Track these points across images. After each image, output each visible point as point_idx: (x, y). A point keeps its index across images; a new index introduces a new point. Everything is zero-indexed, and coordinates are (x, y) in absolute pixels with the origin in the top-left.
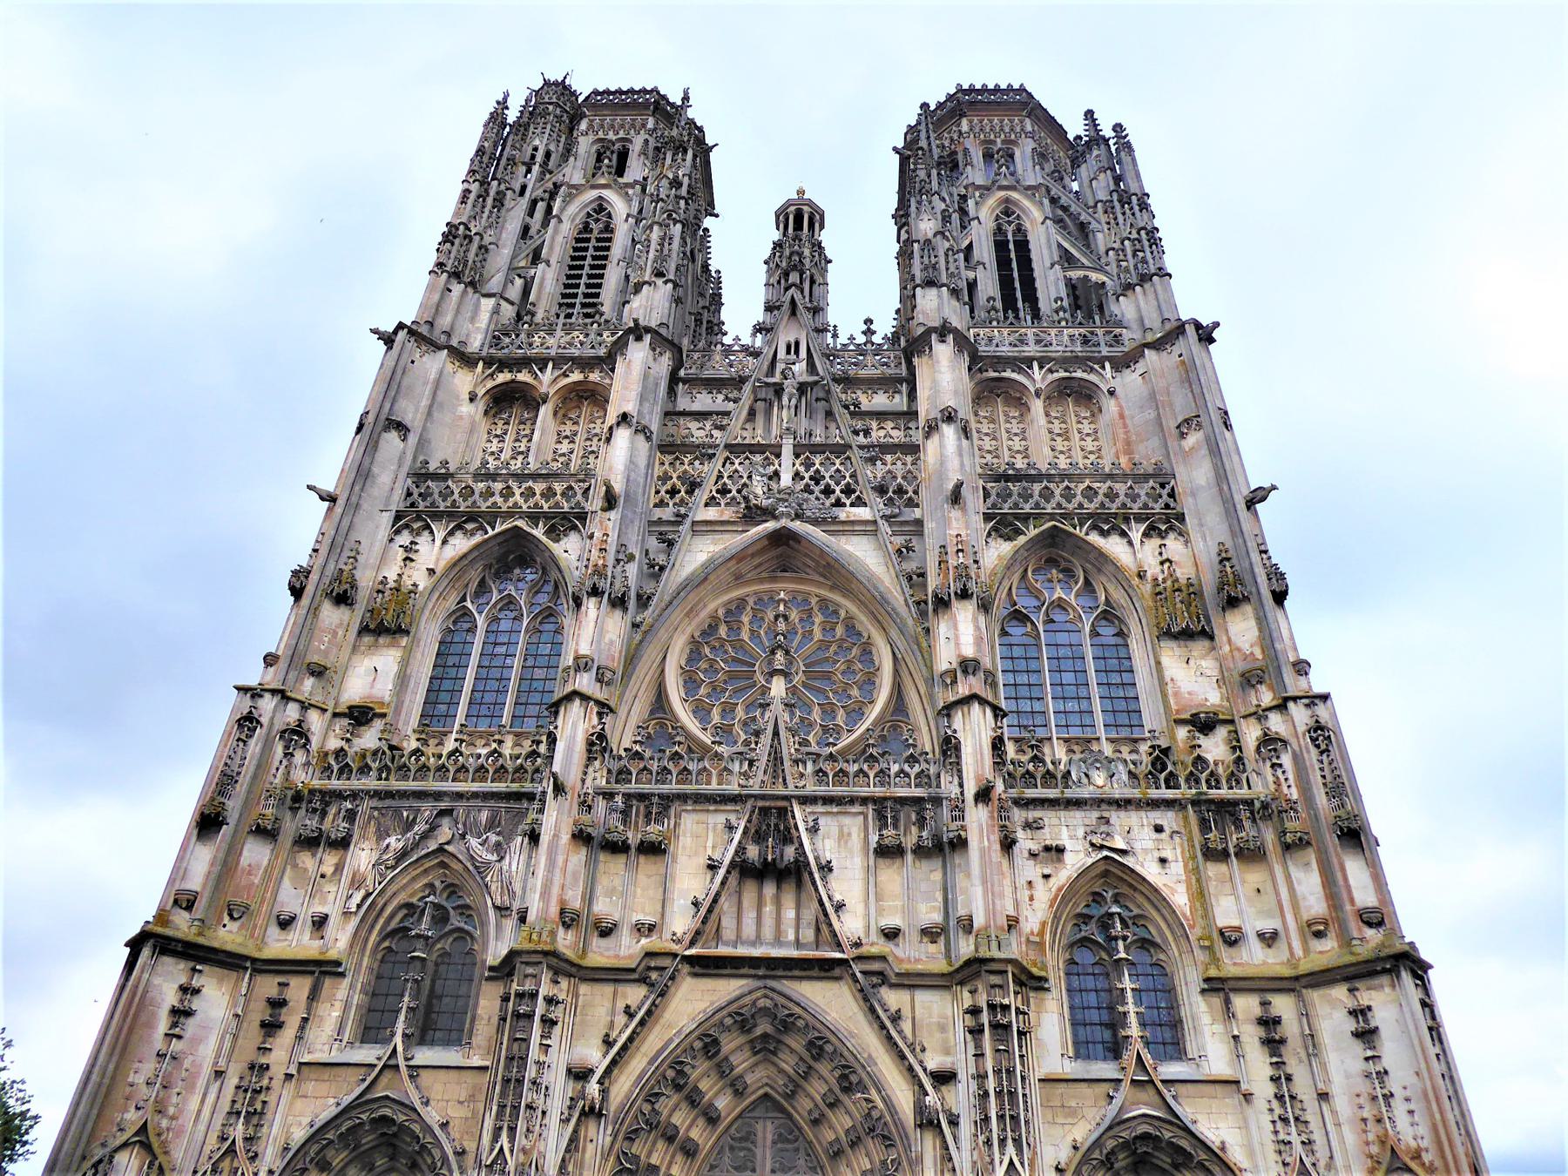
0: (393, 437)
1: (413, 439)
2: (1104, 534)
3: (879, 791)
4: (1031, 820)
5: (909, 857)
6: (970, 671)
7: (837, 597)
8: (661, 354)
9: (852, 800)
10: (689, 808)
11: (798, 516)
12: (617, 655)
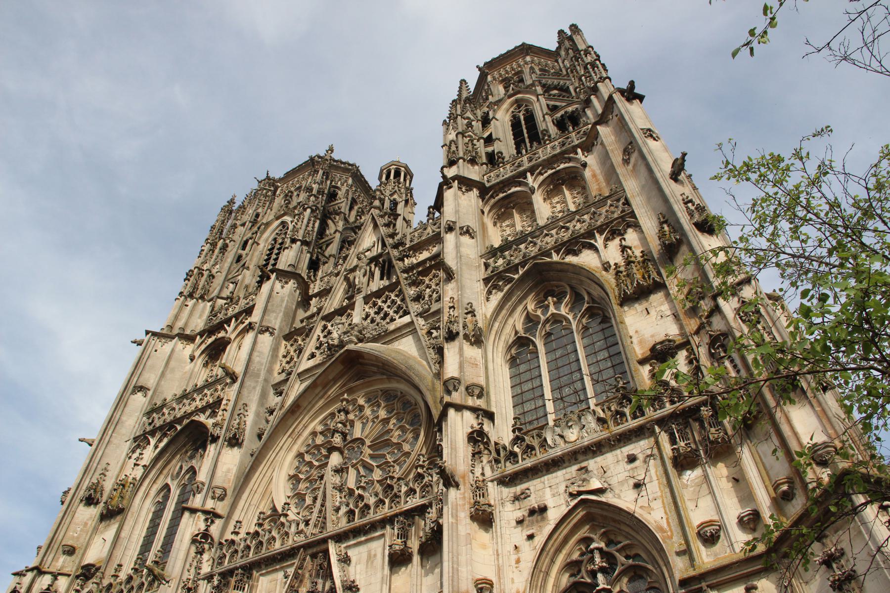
0: (140, 394)
1: (150, 393)
2: (576, 253)
3: (396, 510)
4: (519, 493)
5: (416, 559)
6: (451, 388)
7: (394, 385)
8: (286, 283)
9: (374, 526)
10: (264, 572)
11: (360, 340)
12: (232, 478)
